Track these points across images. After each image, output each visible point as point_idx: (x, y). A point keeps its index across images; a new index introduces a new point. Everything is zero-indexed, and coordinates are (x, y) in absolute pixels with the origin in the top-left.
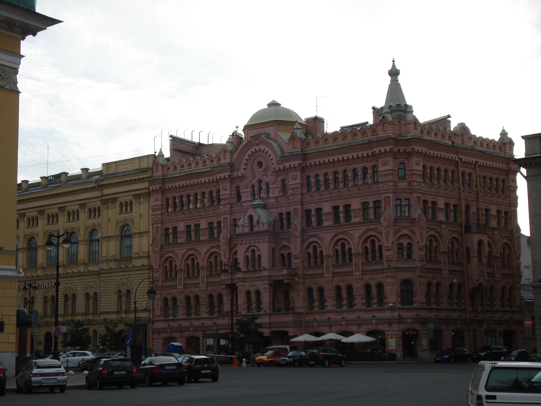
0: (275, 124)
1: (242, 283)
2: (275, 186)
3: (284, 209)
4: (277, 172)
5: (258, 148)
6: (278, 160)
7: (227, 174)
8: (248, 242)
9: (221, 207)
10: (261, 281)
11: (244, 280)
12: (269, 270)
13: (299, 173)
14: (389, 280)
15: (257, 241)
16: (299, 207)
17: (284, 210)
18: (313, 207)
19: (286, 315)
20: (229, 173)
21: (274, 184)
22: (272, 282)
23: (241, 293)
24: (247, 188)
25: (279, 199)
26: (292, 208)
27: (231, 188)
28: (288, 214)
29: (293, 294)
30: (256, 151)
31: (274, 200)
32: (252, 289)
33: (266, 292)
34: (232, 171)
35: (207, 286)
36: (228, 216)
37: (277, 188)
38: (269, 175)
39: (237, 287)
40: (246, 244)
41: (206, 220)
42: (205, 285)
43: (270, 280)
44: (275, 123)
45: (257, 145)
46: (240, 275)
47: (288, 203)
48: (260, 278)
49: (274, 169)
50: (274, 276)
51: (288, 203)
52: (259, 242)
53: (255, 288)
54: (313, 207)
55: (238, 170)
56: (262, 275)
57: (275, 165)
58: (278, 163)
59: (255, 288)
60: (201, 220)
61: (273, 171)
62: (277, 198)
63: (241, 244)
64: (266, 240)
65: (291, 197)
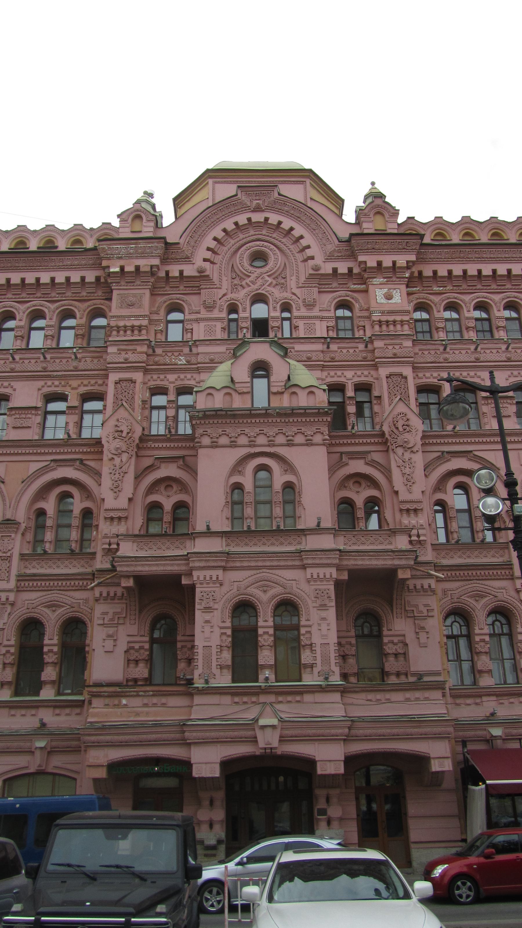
0: (308, 181)
1: (220, 572)
2: (315, 312)
3: (349, 374)
4: (320, 280)
6: (330, 248)
8: (243, 440)
9: (110, 350)
10: (304, 567)
11: (227, 561)
12: (335, 532)
15: (281, 439)
16: (407, 371)
17: (349, 378)
19: (418, 694)
20: (156, 262)
21: (310, 306)
22: (345, 576)
23: (208, 609)
25: (334, 347)
26: (383, 372)
27: (152, 303)
28: (363, 388)
29: (398, 627)
31: (319, 347)
32: (265, 600)
33: (323, 607)
34: (165, 260)
35: (18, 590)
36: (138, 376)
37: (322, 318)
38: (292, 283)
39: (192, 588)
40: (233, 445)
41: (41, 383)
42: (12, 584)
43: (339, 568)
44: (308, 177)
45: (258, 209)
46: (202, 545)
48: (301, 560)
49: (317, 268)
51: (365, 359)
52: (290, 444)
53: (271, 592)
55: (188, 260)
56: (302, 547)
57: (319, 260)
59: (278, 590)
60: (17, 385)
62: (326, 341)
63: (214, 445)
64: (318, 439)
65: (378, 344)
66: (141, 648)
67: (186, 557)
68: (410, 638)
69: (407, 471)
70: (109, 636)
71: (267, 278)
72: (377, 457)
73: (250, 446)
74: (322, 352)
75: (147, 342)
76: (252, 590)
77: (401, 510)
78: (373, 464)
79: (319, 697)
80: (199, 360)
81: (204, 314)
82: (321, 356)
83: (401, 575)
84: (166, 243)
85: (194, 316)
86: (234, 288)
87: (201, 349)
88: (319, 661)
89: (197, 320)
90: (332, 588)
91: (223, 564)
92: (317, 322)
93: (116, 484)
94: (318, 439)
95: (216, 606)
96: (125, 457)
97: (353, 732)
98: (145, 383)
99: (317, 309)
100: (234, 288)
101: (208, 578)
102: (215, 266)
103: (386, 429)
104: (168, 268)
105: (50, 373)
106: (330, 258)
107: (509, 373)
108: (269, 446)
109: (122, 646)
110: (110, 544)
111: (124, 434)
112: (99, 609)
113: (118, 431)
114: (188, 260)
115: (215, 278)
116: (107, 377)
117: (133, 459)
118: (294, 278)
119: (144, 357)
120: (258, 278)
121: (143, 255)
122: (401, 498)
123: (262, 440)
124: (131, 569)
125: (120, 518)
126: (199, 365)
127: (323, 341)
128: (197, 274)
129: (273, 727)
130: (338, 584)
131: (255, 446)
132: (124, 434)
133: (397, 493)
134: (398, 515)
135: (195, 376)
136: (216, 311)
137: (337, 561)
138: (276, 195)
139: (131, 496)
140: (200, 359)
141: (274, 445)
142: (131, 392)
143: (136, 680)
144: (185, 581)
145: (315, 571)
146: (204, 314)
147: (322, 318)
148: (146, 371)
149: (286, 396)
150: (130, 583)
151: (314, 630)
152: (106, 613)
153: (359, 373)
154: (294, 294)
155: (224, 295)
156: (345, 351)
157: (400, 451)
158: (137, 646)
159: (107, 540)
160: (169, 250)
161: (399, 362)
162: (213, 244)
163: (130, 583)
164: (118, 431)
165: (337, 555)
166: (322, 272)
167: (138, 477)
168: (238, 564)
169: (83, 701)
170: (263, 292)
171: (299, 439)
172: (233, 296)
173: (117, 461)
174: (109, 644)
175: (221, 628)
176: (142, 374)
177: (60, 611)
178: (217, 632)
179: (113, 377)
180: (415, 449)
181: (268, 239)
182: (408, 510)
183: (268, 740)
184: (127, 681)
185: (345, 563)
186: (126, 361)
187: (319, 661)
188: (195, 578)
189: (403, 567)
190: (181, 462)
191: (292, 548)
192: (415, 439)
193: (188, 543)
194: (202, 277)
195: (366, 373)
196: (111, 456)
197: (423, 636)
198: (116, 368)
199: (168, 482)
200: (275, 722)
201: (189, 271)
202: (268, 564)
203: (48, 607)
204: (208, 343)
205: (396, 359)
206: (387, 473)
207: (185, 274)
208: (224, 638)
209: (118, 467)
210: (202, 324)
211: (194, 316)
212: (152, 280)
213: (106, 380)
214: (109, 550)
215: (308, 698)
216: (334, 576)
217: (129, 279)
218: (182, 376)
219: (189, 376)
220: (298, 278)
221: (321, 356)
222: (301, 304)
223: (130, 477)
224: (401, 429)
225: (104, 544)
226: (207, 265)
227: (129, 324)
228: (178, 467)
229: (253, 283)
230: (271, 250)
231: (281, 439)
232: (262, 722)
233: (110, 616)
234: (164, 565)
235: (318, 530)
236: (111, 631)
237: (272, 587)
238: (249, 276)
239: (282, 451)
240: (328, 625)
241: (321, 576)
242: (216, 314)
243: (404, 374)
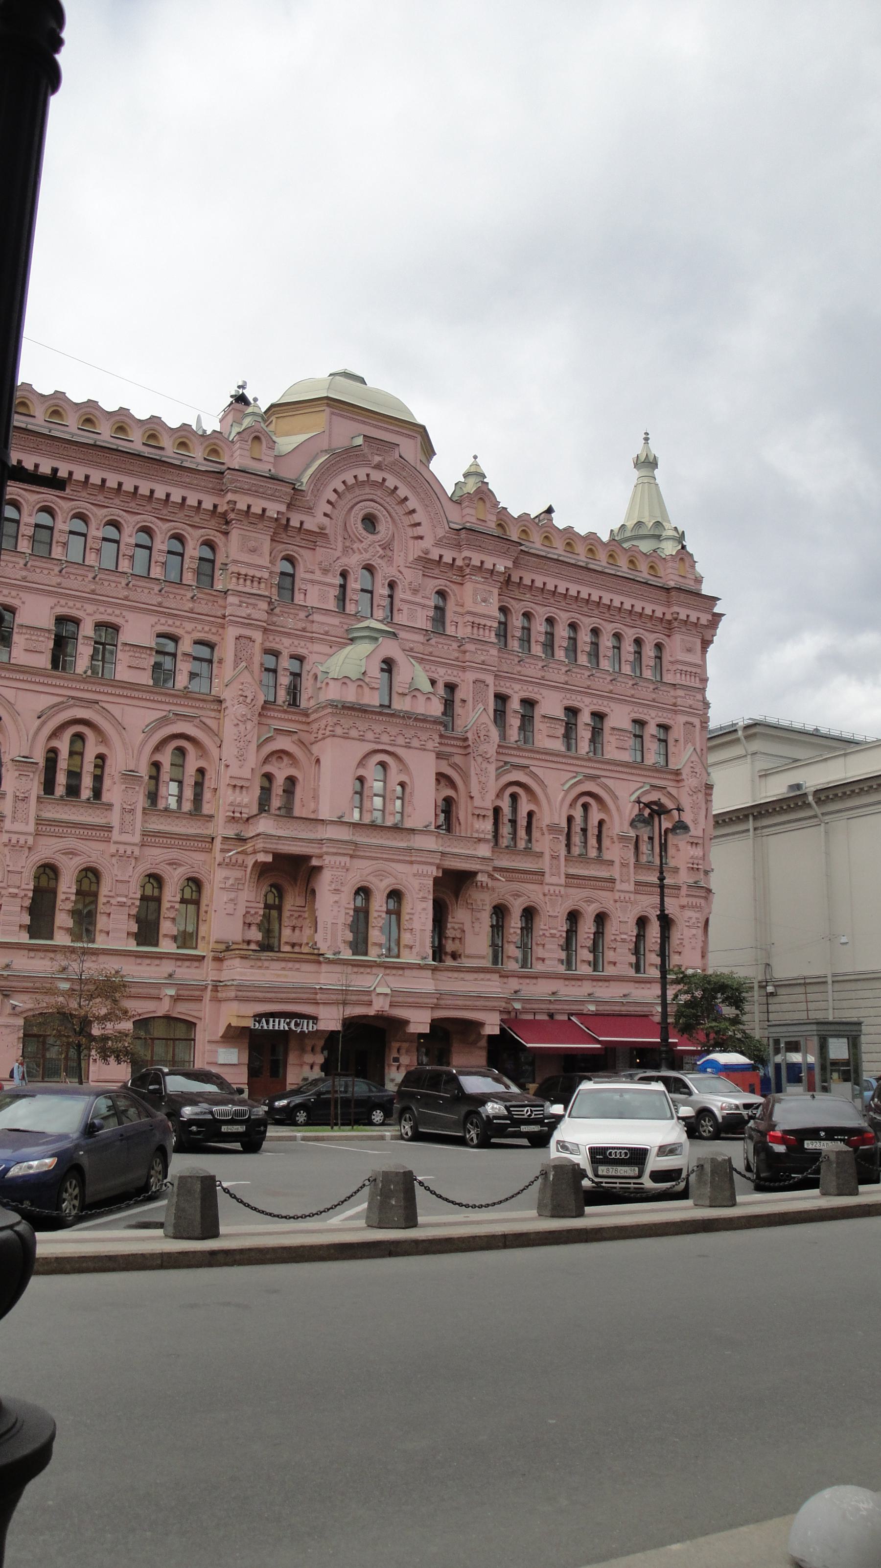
1: (347, 859)
2: (418, 599)
4: (426, 564)
5: (376, 476)
6: (441, 533)
7: (274, 508)
10: (411, 863)
13: (496, 591)
14: (689, 913)
16: (490, 679)
18: (517, 694)
21: (415, 591)
24: (325, 571)
30: (368, 482)
31: (420, 638)
36: (258, 636)
37: (424, 606)
40: (361, 739)
42: (137, 839)
44: (420, 433)
45: (378, 467)
47: (457, 659)
50: (454, 855)
51: (457, 659)
52: (408, 746)
54: (517, 694)
55: (309, 510)
58: (439, 543)
59: (393, 881)
61: (419, 559)
64: (430, 745)
65: (470, 647)
66: (256, 913)
67: (320, 841)
68: (467, 927)
69: (483, 779)
70: (231, 900)
71: (379, 549)
72: (458, 759)
73: (375, 742)
74: (422, 644)
75: (269, 600)
76: (371, 878)
77: (473, 814)
78: (454, 766)
79: (415, 973)
80: (314, 630)
81: (318, 576)
82: (420, 648)
83: (480, 877)
84: (294, 489)
85: (308, 576)
86: (346, 550)
87: (316, 617)
88: (417, 944)
89: (312, 582)
90: (431, 883)
91: (351, 852)
92: (419, 609)
93: (241, 753)
94: (430, 745)
95: (342, 889)
96: (249, 725)
97: (442, 1002)
98: (262, 644)
99: (420, 595)
100: (346, 550)
101: (338, 863)
102: (333, 522)
103: (470, 735)
104: (291, 515)
105: (165, 610)
106: (439, 543)
107: (563, 695)
108: (390, 744)
109: (241, 911)
110: (234, 812)
111: (248, 700)
112: (220, 874)
113: (242, 696)
114: (309, 510)
115: (332, 538)
116: (223, 626)
117: (256, 729)
118: (402, 554)
119: (265, 616)
120: (370, 545)
121: (272, 498)
122: (476, 805)
123: (385, 738)
124: (274, 846)
125: (242, 787)
126: (314, 635)
127: (424, 632)
128: (318, 530)
129: (386, 995)
130: (436, 881)
131: (379, 743)
132: (248, 700)
133: (472, 798)
134: (470, 816)
135: (309, 645)
136: (330, 574)
137: (438, 861)
138: (397, 456)
139: (254, 767)
140: (315, 627)
141: (395, 745)
142: (250, 651)
143: (249, 942)
144: (315, 862)
145: (421, 868)
146: (318, 576)
147: (424, 606)
148: (265, 630)
149: (408, 699)
150: (269, 859)
151: (415, 917)
152: (227, 878)
153: (449, 672)
154: (400, 572)
155: (338, 558)
156: (440, 646)
157: (479, 759)
158: (253, 911)
159: (232, 808)
160: (296, 497)
161: (485, 669)
162: (333, 497)
163: (269, 859)
164: (242, 696)
165: (439, 856)
166: (430, 556)
167: (259, 746)
168: (362, 854)
169: (204, 957)
170: (373, 563)
171: (415, 743)
172: (344, 561)
173: (242, 727)
174: (230, 907)
175: (346, 908)
176: (261, 633)
177: (181, 870)
178: (343, 911)
179: (232, 632)
180: (490, 760)
181: (382, 502)
182: (478, 815)
183: (379, 1006)
184: (244, 941)
185: (443, 863)
186: (249, 617)
187: (417, 944)
188: (326, 862)
189: (482, 872)
190: (295, 737)
191: (403, 845)
192: (491, 749)
193: (320, 828)
194: (321, 534)
195: (455, 673)
196: (236, 722)
197: (477, 925)
198: (237, 622)
199: (281, 754)
200: (388, 991)
201: (311, 524)
202: (385, 856)
203: (170, 864)
204: (324, 612)
205: (483, 666)
206: (466, 777)
207: (305, 526)
208: (347, 916)
209: (243, 734)
210: (317, 587)
211: (308, 576)
212: (273, 525)
213: (220, 630)
214: (233, 818)
215: (407, 972)
216: (435, 874)
217: (252, 520)
218: (296, 642)
219: (302, 643)
220: (406, 555)
221: (420, 648)
222: (407, 586)
223: (253, 746)
224: (482, 738)
225: (228, 811)
226: (326, 520)
227: (251, 572)
228: (293, 742)
229: (366, 551)
230: (384, 516)
231: (401, 740)
232: (379, 990)
233: (231, 881)
234: (302, 846)
235: (424, 832)
236: (232, 895)
237: (387, 877)
238: (362, 542)
239: (400, 751)
240: (427, 914)
241: (425, 872)
242: (329, 579)
243: (487, 682)
